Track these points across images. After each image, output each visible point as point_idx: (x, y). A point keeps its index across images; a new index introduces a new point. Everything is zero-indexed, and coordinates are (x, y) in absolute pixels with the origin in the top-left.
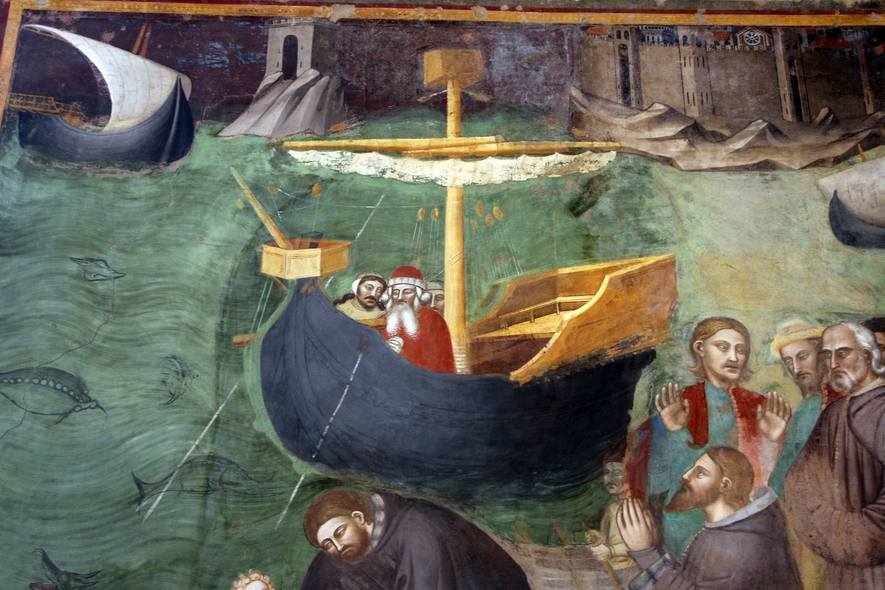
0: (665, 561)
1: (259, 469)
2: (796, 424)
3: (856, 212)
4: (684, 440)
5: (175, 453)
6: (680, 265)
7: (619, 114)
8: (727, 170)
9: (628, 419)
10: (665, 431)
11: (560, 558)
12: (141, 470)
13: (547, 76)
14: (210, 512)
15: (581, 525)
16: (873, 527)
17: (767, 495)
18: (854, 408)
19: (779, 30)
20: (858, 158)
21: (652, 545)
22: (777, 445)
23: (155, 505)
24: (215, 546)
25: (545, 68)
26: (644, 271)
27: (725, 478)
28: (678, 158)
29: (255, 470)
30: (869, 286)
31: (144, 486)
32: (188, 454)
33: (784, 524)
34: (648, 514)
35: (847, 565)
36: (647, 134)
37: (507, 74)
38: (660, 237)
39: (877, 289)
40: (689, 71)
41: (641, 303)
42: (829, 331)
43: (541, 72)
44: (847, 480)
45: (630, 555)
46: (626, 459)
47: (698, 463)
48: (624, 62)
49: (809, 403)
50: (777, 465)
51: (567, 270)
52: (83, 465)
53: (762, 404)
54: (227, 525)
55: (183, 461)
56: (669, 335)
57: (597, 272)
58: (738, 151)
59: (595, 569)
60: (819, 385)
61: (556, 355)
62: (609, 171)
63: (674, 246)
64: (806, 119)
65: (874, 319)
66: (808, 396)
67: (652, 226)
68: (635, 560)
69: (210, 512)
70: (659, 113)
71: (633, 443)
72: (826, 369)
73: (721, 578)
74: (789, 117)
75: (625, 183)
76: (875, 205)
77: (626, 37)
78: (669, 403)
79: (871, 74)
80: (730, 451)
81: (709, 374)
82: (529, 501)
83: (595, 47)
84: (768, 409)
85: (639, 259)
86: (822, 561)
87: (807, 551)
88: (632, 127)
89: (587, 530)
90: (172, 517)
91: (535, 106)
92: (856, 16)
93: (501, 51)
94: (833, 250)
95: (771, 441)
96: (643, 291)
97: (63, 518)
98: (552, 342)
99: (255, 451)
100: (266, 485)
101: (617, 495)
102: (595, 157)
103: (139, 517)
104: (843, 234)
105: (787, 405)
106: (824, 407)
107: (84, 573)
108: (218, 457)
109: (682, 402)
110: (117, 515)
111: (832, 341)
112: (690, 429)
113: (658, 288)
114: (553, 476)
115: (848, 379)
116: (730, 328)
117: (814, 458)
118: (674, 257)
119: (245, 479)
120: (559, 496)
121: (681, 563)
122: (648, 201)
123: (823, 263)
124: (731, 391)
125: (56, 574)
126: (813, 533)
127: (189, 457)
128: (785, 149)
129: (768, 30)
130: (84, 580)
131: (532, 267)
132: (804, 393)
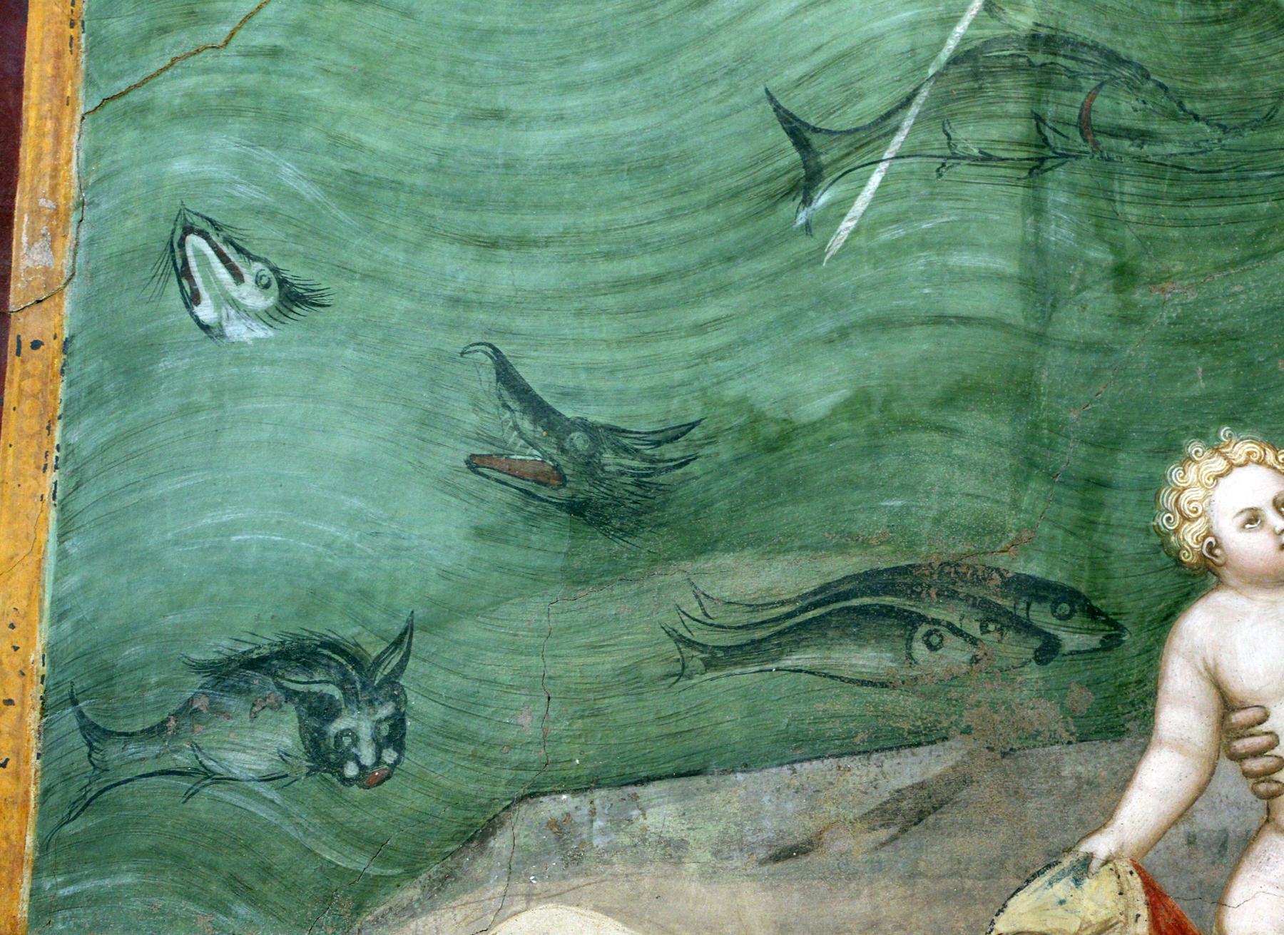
1: (1223, 85)
5: (914, 26)
12: (799, 83)
14: (1059, 233)
23: (860, 206)
24: (1089, 347)
29: (1209, 86)
31: (816, 140)
32: (960, 30)
52: (593, 65)
54: (1123, 275)
55: (945, 55)
69: (1059, 233)
90: (923, 244)
97: (547, 242)
99: (1201, 21)
100: (1249, 137)
103: (804, 245)
107: (644, 427)
108: (1067, 42)
110: (732, 236)
119: (1174, 116)
125: (550, 427)
127: (964, 40)
130: (648, 451)
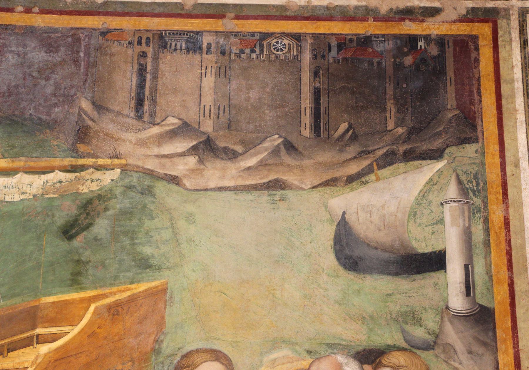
6: (172, 292)
7: (128, 129)
8: (235, 189)
13: (57, 86)
19: (308, 38)
20: (372, 177)
25: (55, 77)
26: (132, 299)
28: (185, 176)
30: (365, 315)
36: (156, 151)
37: (13, 84)
39: (372, 317)
40: (209, 82)
41: (124, 334)
42: (316, 363)
43: (52, 82)
48: (142, 71)
57: (82, 300)
58: (249, 168)
62: (110, 190)
63: (168, 272)
64: (324, 134)
65: (364, 350)
67: (147, 250)
70: (171, 127)
74: (307, 132)
75: (126, 204)
76: (382, 228)
77: (148, 44)
79: (398, 85)
83: (113, 55)
85: (129, 286)
88: (141, 143)
91: (40, 119)
92: (390, 24)
93: (10, 57)
94: (332, 276)
96: (129, 321)
102: (98, 175)
104: (345, 258)
113: (145, 318)
116: (215, 361)
118: (167, 284)
122: (147, 223)
123: (321, 290)
128: (298, 167)
129: (298, 38)
131: (13, 296)
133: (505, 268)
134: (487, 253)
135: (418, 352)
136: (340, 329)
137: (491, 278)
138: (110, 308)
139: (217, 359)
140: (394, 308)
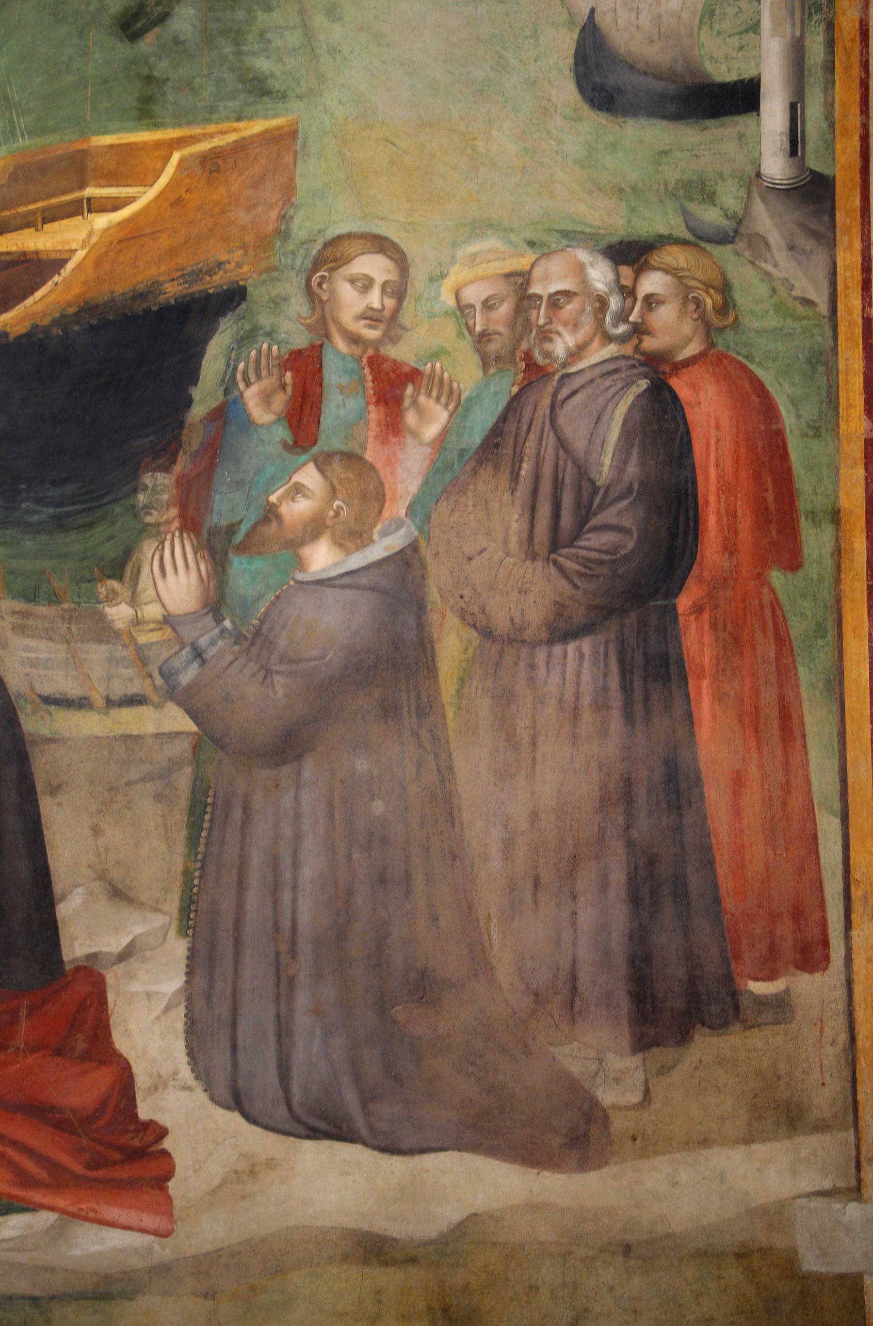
0: (223, 631)
2: (465, 416)
3: (622, 50)
4: (278, 439)
6: (306, 139)
9: (188, 402)
10: (248, 423)
11: (52, 622)
15: (92, 571)
16: (563, 583)
17: (403, 531)
18: (564, 393)
21: (205, 605)
22: (429, 450)
26: (241, 146)
27: (337, 503)
30: (623, 185)
33: (423, 578)
34: (204, 557)
35: (512, 641)
38: (277, 85)
39: (635, 189)
41: (230, 204)
42: (543, 261)
44: (533, 509)
45: (168, 620)
46: (177, 468)
47: (296, 478)
49: (492, 384)
50: (426, 483)
51: (108, 140)
53: (414, 384)
56: (274, 261)
57: (158, 144)
59: (108, 642)
60: (513, 354)
61: (76, 290)
63: (299, 103)
65: (621, 243)
66: (492, 371)
67: (263, 65)
68: (174, 629)
71: (193, 442)
72: (528, 325)
73: (310, 660)
76: (656, 38)
78: (259, 377)
80: (352, 458)
81: (333, 329)
82: (8, 532)
84: (423, 391)
85: (235, 124)
86: (473, 634)
87: (453, 620)
89: (100, 581)
94: (571, 119)
95: (421, 444)
98: (70, 266)
101: (157, 525)
104: (593, 89)
105: (455, 385)
106: (515, 390)
109: (282, 376)
111: (546, 278)
112: (289, 421)
113: (262, 179)
114: (53, 493)
115: (560, 347)
116: (378, 252)
117: (486, 473)
118: (297, 123)
120: (60, 524)
121: (249, 636)
122: (262, 17)
123: (553, 142)
124: (365, 361)
126: (467, 592)
131: (45, 131)
132: (485, 367)
133: (856, 110)
134: (829, 84)
135: (708, 247)
136: (582, 207)
137: (832, 125)
138: (204, 159)
139: (381, 250)
140: (672, 175)
